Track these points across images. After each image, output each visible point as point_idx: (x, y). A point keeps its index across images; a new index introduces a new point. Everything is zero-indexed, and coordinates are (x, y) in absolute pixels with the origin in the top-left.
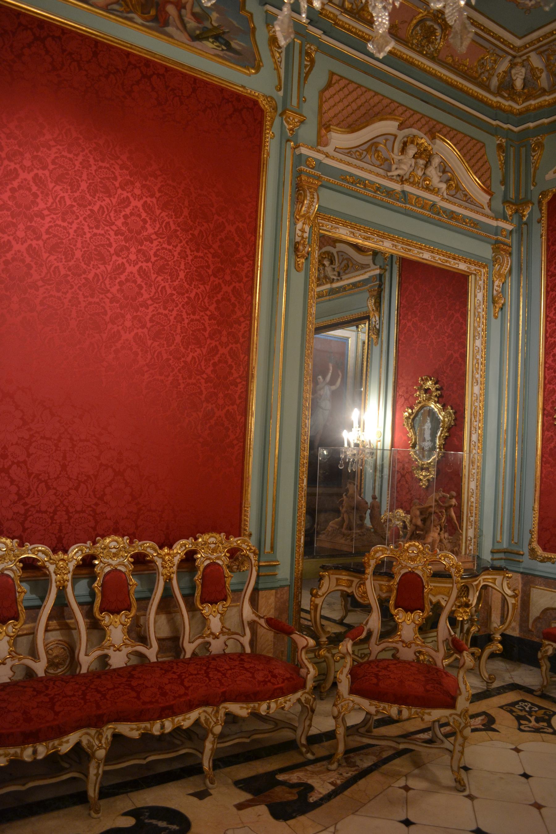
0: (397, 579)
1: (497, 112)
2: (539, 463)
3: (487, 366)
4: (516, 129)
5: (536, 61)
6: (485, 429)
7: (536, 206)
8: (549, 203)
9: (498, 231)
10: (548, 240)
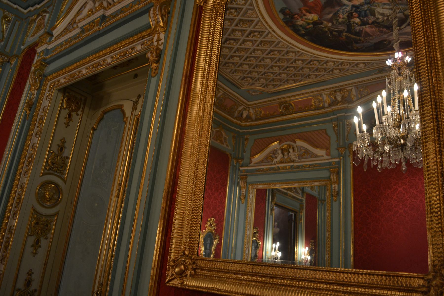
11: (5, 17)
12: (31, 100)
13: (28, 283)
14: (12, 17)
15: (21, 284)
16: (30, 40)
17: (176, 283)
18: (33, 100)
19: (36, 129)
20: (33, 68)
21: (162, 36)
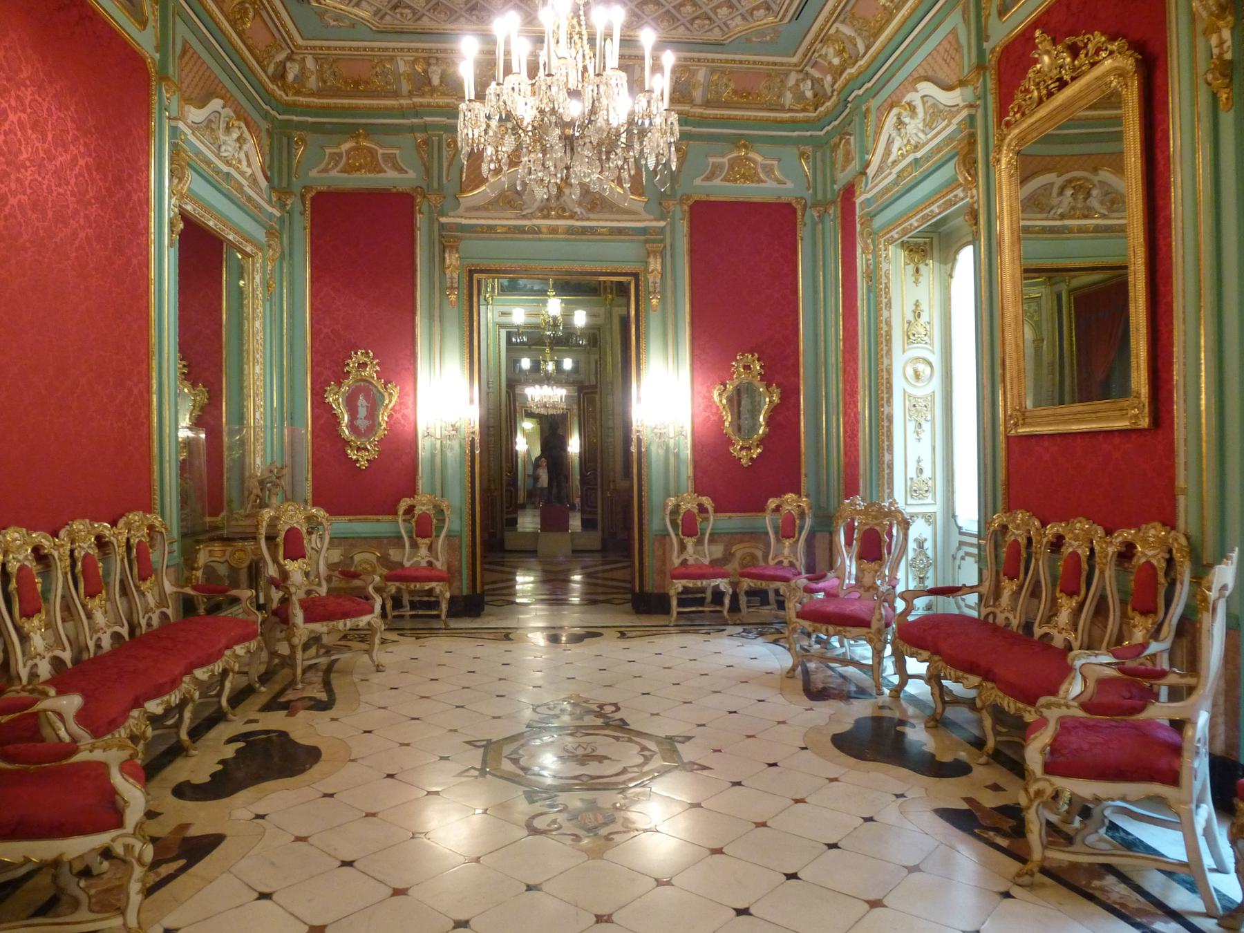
1: (270, 98)
4: (279, 117)
5: (310, 63)
8: (313, 199)
12: (868, 266)
14: (809, 149)
15: (912, 473)
16: (843, 178)
19: (884, 301)
21: (974, 191)
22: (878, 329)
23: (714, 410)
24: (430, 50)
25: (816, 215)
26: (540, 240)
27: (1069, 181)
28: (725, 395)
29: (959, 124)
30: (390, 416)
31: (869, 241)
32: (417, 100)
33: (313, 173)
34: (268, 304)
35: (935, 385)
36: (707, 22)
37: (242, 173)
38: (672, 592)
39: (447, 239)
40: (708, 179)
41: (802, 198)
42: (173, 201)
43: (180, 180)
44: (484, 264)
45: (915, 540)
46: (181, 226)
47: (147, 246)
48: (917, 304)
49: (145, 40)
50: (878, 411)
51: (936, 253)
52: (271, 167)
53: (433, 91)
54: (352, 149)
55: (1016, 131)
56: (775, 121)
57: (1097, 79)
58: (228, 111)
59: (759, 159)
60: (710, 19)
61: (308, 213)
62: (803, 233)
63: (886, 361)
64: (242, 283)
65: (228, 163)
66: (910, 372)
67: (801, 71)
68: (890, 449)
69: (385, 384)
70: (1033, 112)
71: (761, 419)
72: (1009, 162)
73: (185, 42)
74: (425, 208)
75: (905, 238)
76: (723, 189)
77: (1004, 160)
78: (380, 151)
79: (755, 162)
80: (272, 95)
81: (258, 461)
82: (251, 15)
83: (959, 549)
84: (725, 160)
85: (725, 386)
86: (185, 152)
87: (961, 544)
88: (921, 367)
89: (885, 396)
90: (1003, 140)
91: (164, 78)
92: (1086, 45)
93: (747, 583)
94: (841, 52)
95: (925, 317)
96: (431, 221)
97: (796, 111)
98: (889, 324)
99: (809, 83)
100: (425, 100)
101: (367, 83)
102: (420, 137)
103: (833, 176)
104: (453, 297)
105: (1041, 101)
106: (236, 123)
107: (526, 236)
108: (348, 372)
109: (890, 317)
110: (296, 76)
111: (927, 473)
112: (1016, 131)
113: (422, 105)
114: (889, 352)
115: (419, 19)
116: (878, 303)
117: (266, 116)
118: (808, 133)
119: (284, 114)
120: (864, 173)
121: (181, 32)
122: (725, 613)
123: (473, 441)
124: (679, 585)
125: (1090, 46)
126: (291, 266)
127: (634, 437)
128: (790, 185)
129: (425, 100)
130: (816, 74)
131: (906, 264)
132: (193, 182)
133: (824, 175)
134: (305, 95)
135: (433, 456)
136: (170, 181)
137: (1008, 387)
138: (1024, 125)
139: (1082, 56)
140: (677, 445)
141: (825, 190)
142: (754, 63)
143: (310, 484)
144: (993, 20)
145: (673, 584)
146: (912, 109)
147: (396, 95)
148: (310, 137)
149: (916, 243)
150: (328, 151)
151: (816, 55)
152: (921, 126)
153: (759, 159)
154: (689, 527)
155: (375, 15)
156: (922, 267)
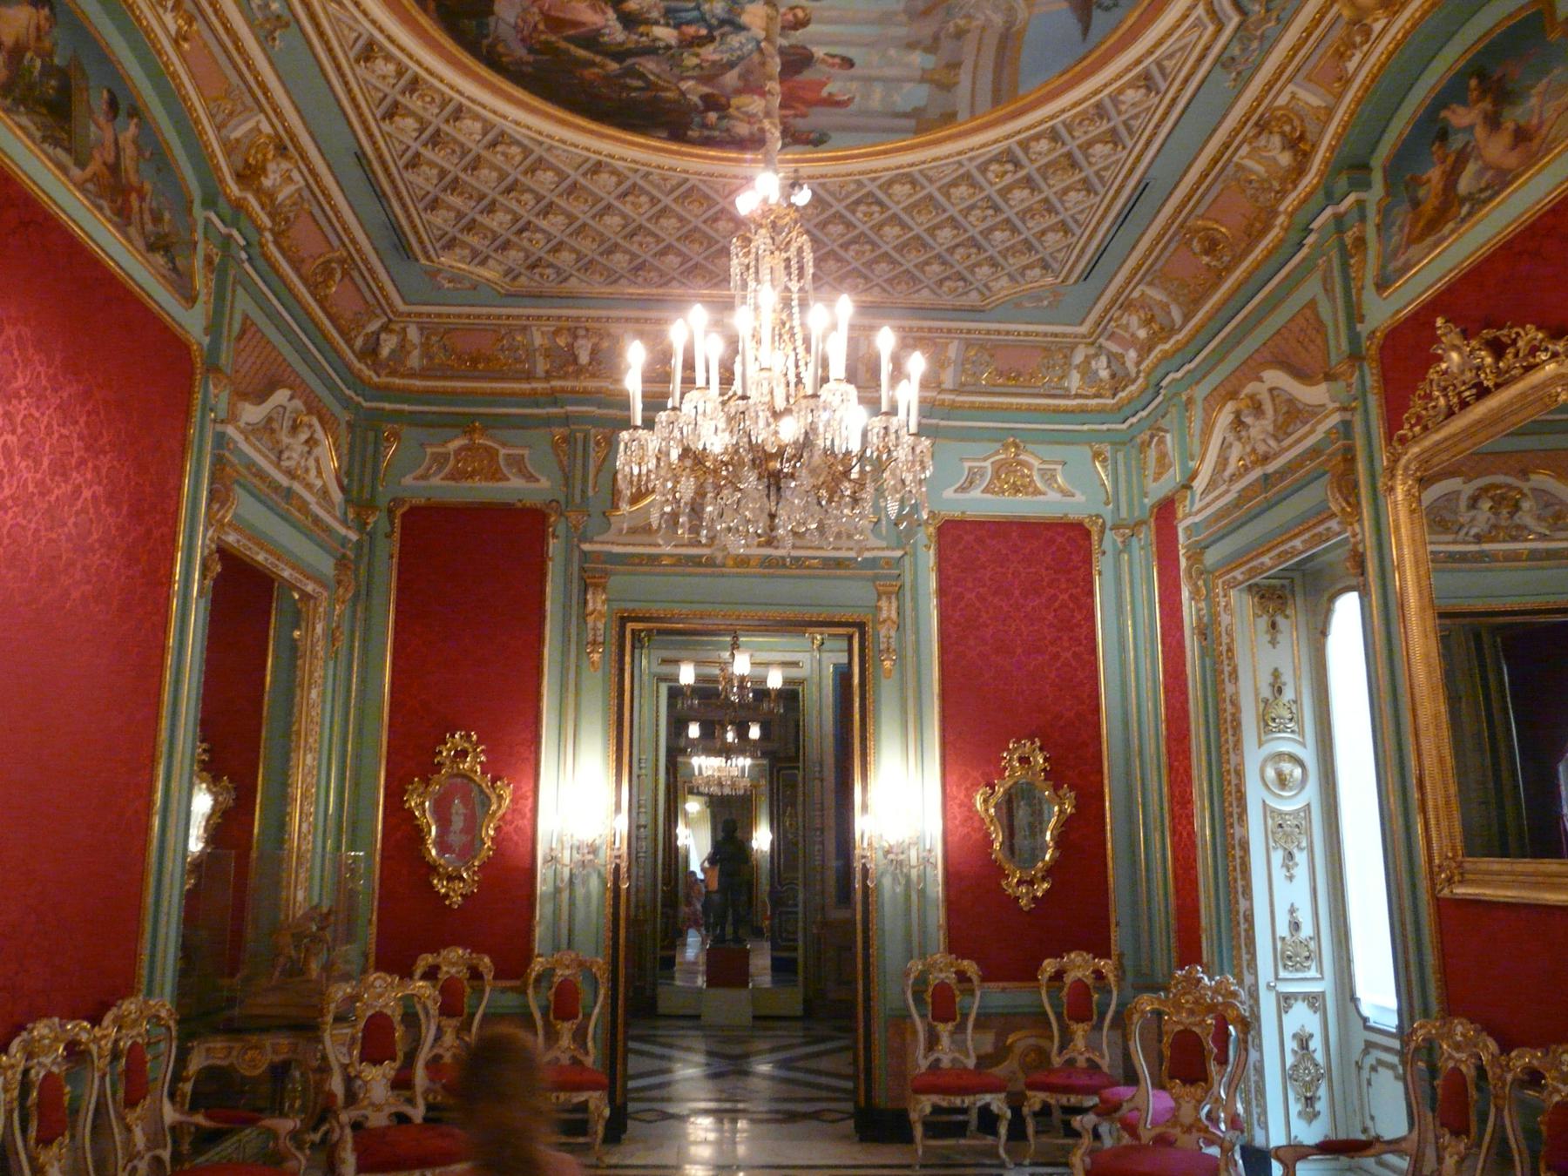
0: (362, 1024)
1: (356, 381)
2: (378, 858)
3: (322, 725)
4: (365, 404)
5: (413, 334)
6: (316, 812)
7: (385, 514)
8: (404, 515)
9: (345, 541)
10: (400, 564)
11: (1097, 455)
12: (1200, 619)
13: (1295, 926)
14: (1107, 449)
15: (1283, 929)
16: (1158, 490)
17: (1446, 892)
18: (1205, 620)
19: (1227, 669)
20: (1183, 563)
21: (1357, 527)
22: (1219, 712)
23: (977, 825)
24: (578, 319)
25: (1119, 540)
26: (723, 575)
27: (1485, 490)
28: (992, 801)
29: (1328, 432)
30: (497, 829)
31: (1200, 583)
32: (556, 383)
33: (408, 480)
34: (331, 664)
35: (1311, 794)
36: (961, 284)
37: (309, 486)
38: (914, 1116)
39: (591, 575)
40: (962, 489)
41: (1098, 516)
42: (210, 533)
43: (223, 505)
44: (641, 608)
45: (1294, 1036)
46: (219, 568)
47: (168, 599)
48: (1276, 674)
49: (192, 322)
50: (1224, 835)
51: (1299, 601)
52: (348, 474)
53: (579, 372)
54: (462, 448)
55: (1416, 450)
56: (1056, 410)
57: (1534, 388)
58: (298, 404)
59: (1036, 463)
60: (964, 279)
61: (397, 536)
62: (1103, 567)
63: (1233, 758)
64: (297, 633)
65: (290, 474)
66: (1270, 773)
67: (1093, 344)
68: (1248, 892)
69: (494, 781)
70: (1439, 426)
71: (1048, 837)
72: (1408, 493)
73: (246, 317)
74: (561, 529)
75: (1257, 580)
76: (981, 503)
77: (1400, 491)
78: (503, 451)
79: (1030, 468)
80: (359, 377)
81: (300, 895)
82: (338, 276)
83: (1366, 1052)
84: (988, 464)
85: (993, 788)
86: (233, 466)
87: (1369, 1046)
88: (1287, 767)
89: (1235, 810)
90: (1396, 461)
91: (213, 368)
92: (1514, 342)
93: (1036, 1099)
94: (1147, 322)
95: (1289, 694)
96: (569, 549)
97: (1086, 397)
98: (1235, 703)
99: (1104, 359)
100: (569, 384)
101: (488, 360)
102: (558, 432)
103: (1141, 486)
104: (596, 657)
105: (1450, 413)
106: (306, 419)
107: (701, 570)
108: (440, 765)
109: (1237, 693)
110: (393, 352)
111: (1307, 930)
112: (1416, 450)
113: (563, 390)
114: (1238, 744)
115: (566, 279)
116: (1217, 673)
117: (347, 403)
118: (1104, 427)
119: (371, 401)
120: (1187, 486)
121: (243, 303)
122: (1002, 1151)
123: (617, 868)
124: (926, 1103)
125: (1520, 343)
126: (367, 609)
127: (858, 865)
128: (1080, 498)
129: (569, 384)
130: (1114, 347)
131: (1256, 616)
132: (244, 506)
133: (1129, 482)
134: (403, 376)
135: (557, 890)
136: (209, 506)
137: (1432, 822)
138: (1427, 443)
139: (1510, 356)
140: (923, 877)
141: (1130, 504)
142: (1027, 334)
143: (374, 930)
144: (1370, 293)
145: (918, 1102)
146: (1258, 409)
147: (529, 376)
148: (409, 433)
149: (1269, 587)
150: (429, 450)
151: (1113, 324)
152: (1270, 428)
153: (1036, 463)
154: (943, 1006)
155: (506, 275)
156: (1280, 619)
